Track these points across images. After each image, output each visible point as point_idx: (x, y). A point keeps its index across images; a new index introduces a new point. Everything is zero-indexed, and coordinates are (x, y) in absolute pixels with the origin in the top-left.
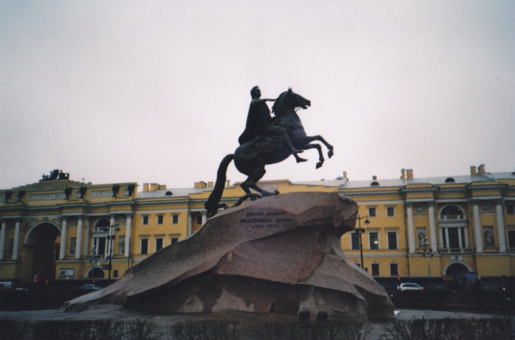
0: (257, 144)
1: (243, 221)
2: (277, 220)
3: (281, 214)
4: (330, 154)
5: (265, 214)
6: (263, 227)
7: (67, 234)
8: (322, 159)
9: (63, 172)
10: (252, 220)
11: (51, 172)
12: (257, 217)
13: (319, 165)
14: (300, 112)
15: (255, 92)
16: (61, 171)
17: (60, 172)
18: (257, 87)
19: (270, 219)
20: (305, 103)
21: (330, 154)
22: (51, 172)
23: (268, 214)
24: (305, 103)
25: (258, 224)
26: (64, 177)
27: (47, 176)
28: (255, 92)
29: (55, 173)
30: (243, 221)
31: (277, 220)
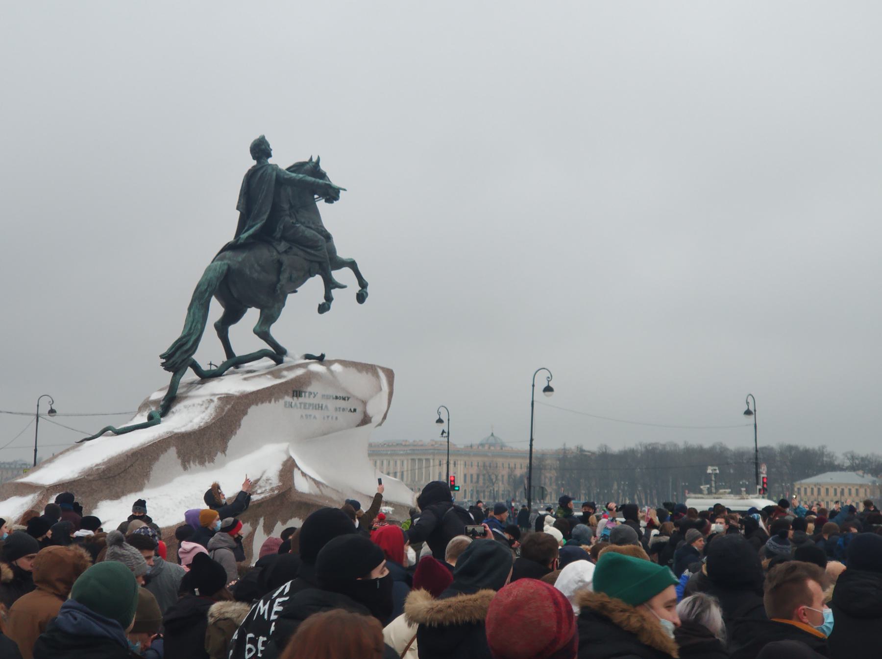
0: (285, 259)
3: (344, 399)
4: (361, 298)
5: (319, 396)
6: (315, 417)
8: (329, 298)
10: (300, 404)
13: (323, 309)
14: (321, 205)
15: (260, 150)
19: (326, 406)
20: (331, 194)
21: (361, 298)
23: (323, 396)
24: (331, 194)
28: (260, 150)
31: (336, 409)
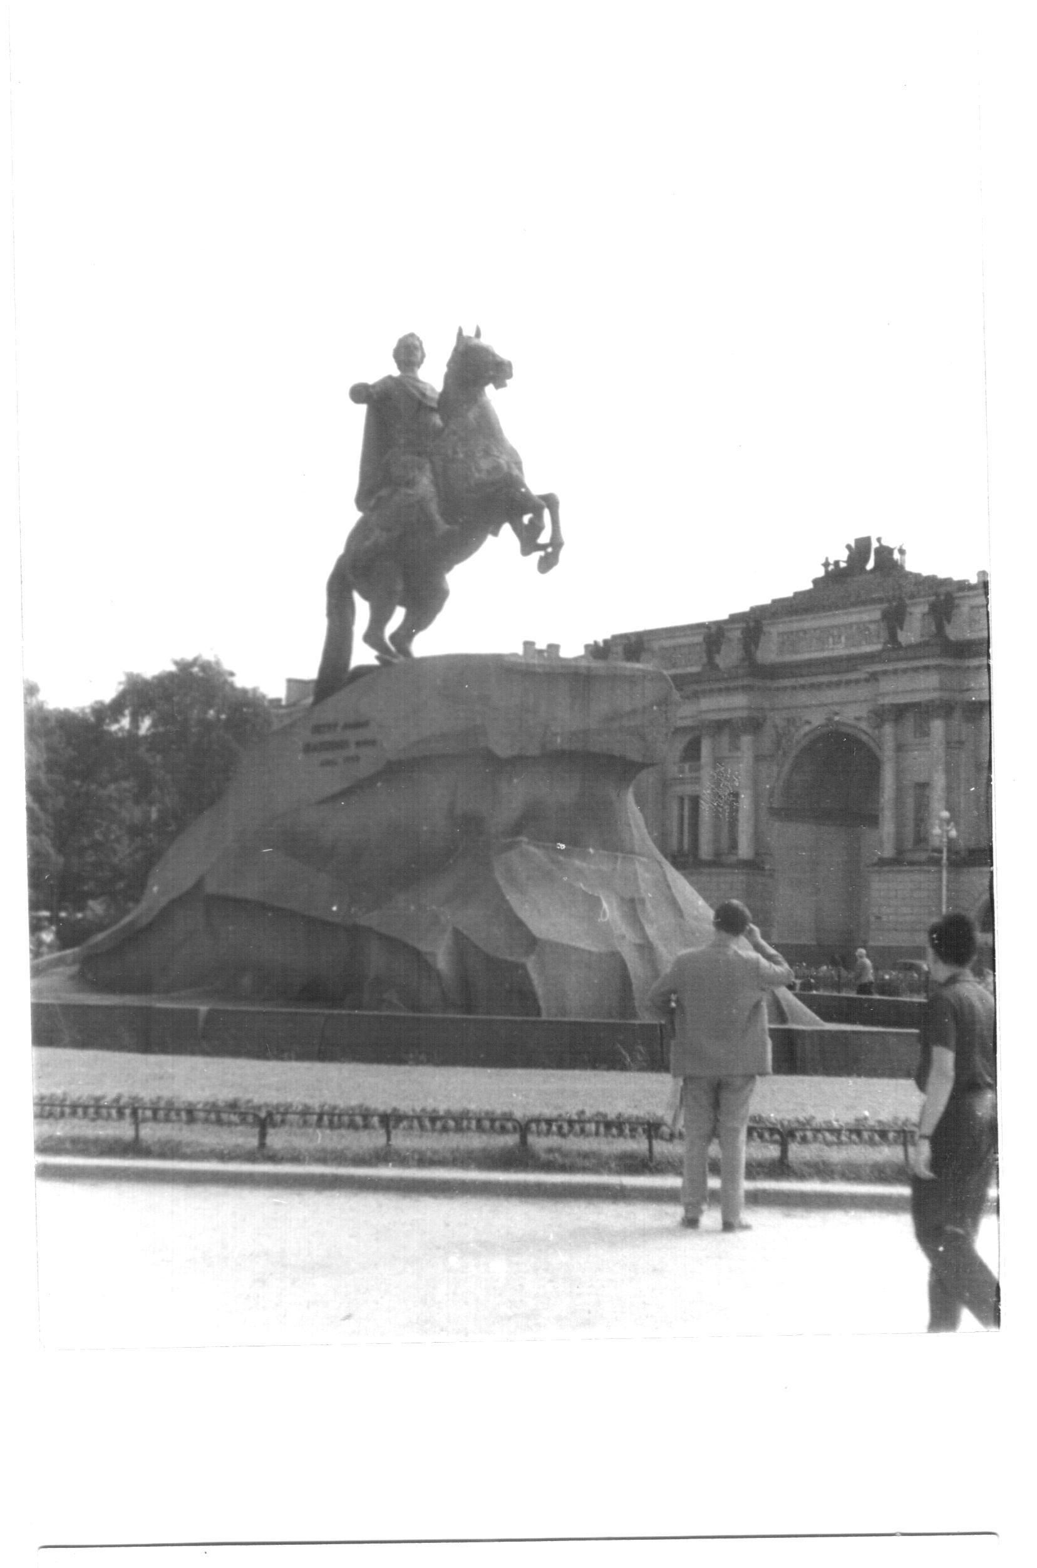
1: (308, 749)
2: (358, 744)
7: (899, 774)
9: (884, 543)
11: (848, 547)
12: (327, 737)
16: (879, 540)
17: (875, 545)
18: (412, 335)
22: (848, 547)
23: (347, 726)
25: (328, 755)
26: (886, 559)
27: (837, 563)
29: (860, 550)
30: (308, 749)
